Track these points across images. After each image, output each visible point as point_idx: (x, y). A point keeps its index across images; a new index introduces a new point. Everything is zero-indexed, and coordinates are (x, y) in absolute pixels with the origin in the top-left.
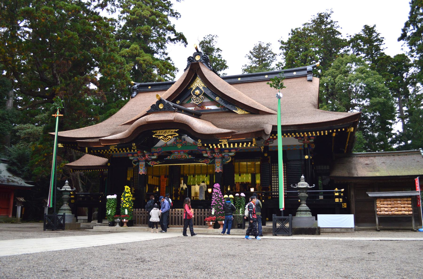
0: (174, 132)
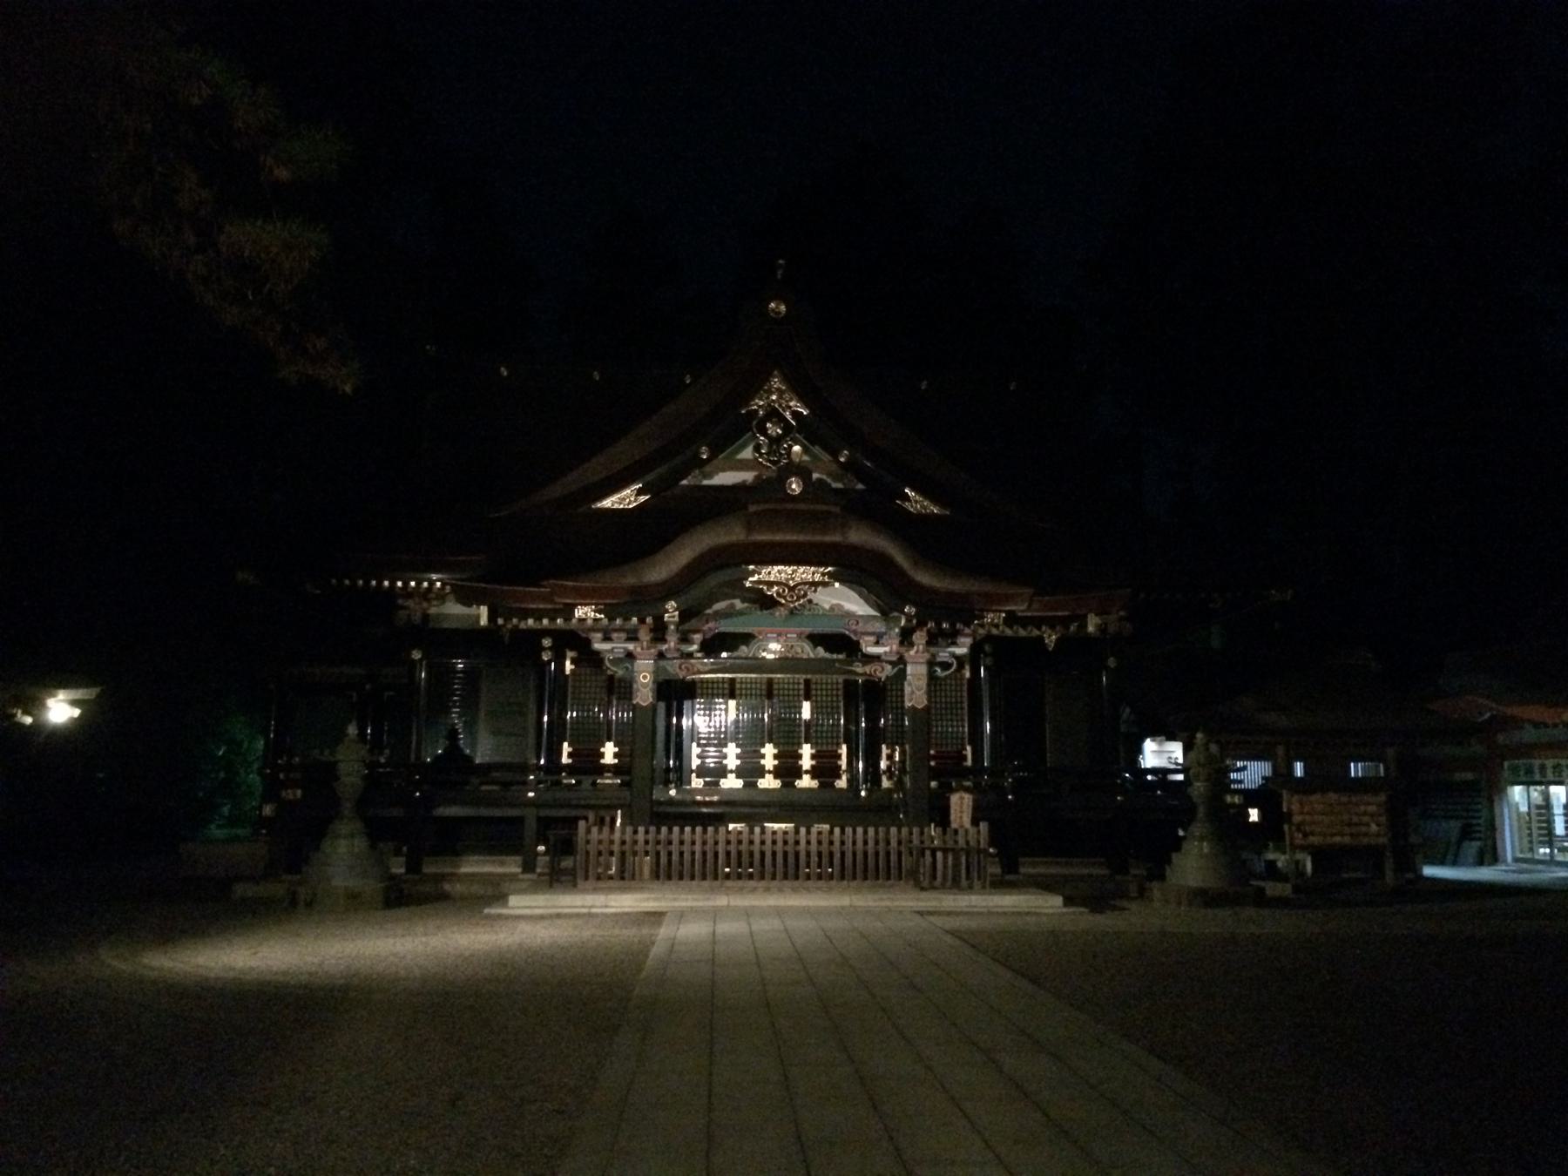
0: (823, 574)
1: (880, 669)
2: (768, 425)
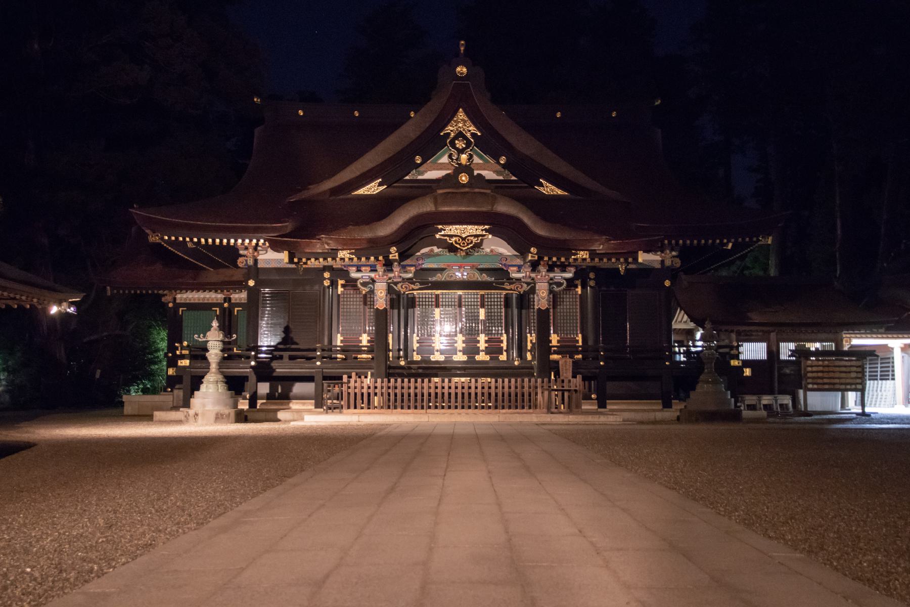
0: (482, 230)
1: (520, 287)
2: (457, 142)
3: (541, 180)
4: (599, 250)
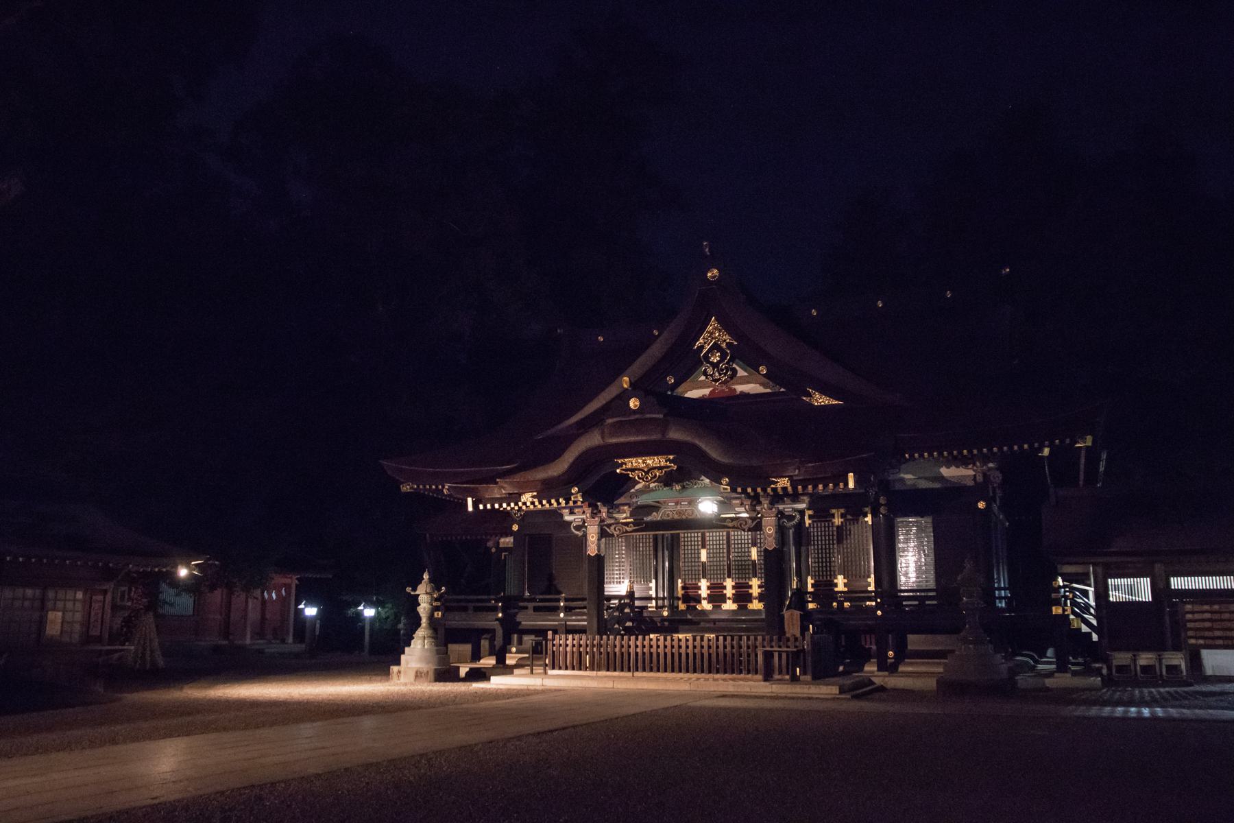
1: (744, 523)
3: (808, 389)
4: (795, 475)
